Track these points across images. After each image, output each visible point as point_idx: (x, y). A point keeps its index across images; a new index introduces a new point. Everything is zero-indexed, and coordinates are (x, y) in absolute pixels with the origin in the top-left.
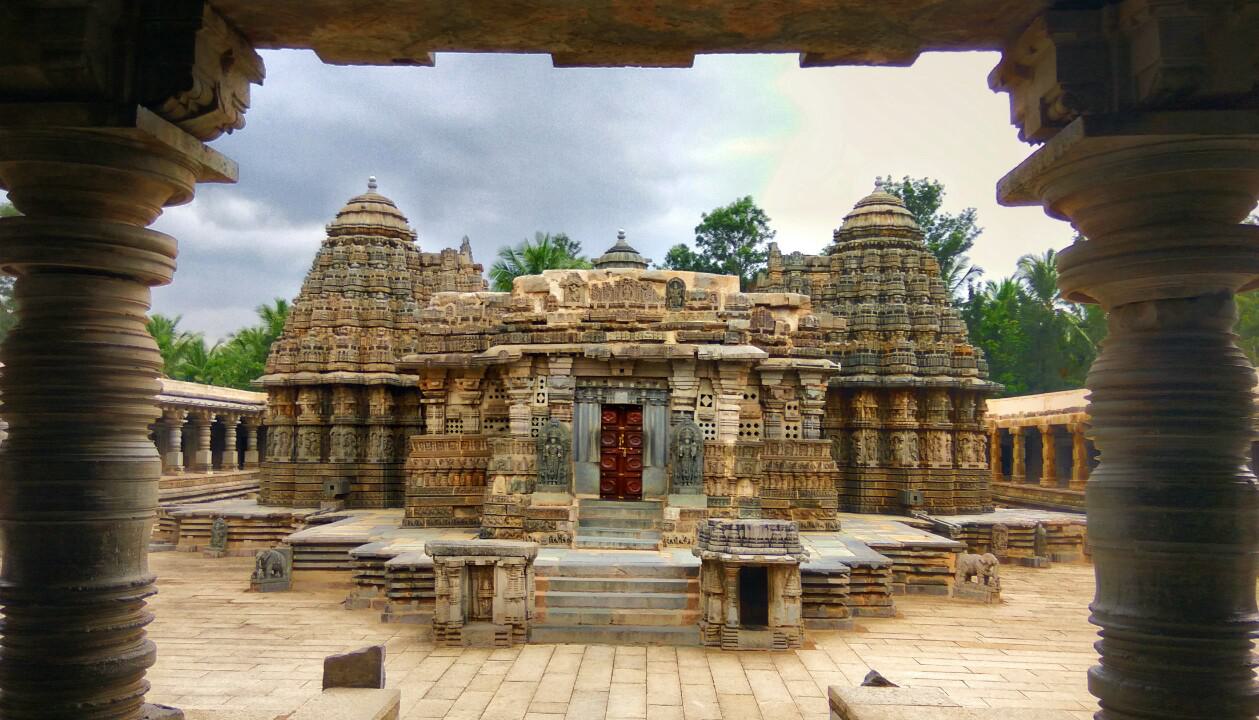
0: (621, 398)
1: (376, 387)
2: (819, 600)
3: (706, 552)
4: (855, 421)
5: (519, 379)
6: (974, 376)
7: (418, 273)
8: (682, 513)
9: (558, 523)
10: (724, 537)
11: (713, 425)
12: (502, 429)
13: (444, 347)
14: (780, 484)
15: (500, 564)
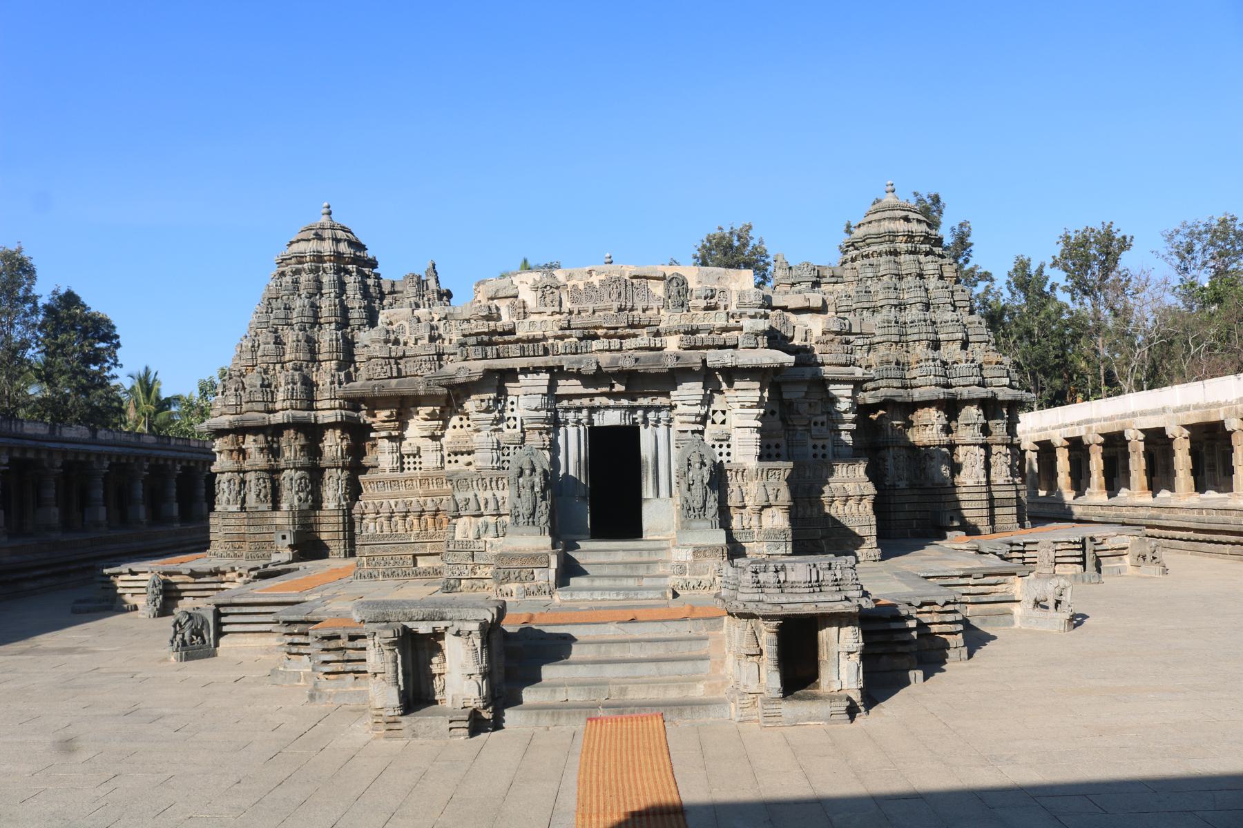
0: (612, 419)
1: (333, 426)
2: (879, 650)
3: (735, 603)
4: (881, 440)
5: (482, 401)
6: (1005, 386)
7: (378, 301)
8: (697, 551)
9: (535, 570)
10: (758, 582)
11: (729, 446)
12: (469, 464)
13: (395, 370)
14: (809, 512)
15: (453, 630)
